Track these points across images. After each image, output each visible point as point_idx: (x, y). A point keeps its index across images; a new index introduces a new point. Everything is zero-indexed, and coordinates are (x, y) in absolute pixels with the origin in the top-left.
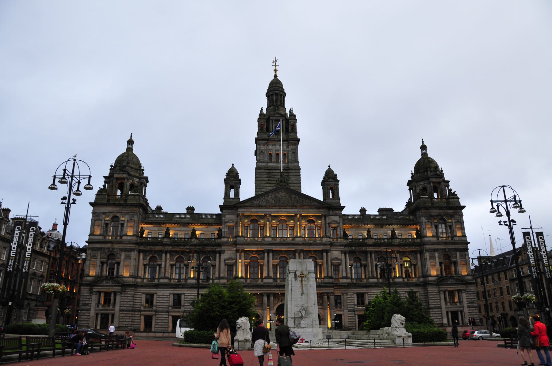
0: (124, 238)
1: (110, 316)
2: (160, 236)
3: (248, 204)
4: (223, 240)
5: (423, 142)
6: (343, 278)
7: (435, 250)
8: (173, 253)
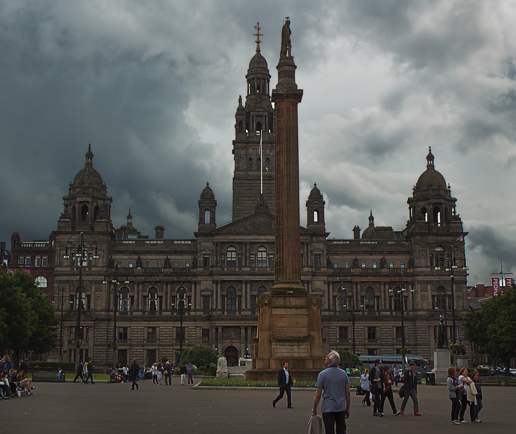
0: (93, 269)
1: (84, 351)
3: (225, 231)
5: (430, 150)
7: (429, 282)
8: (146, 284)
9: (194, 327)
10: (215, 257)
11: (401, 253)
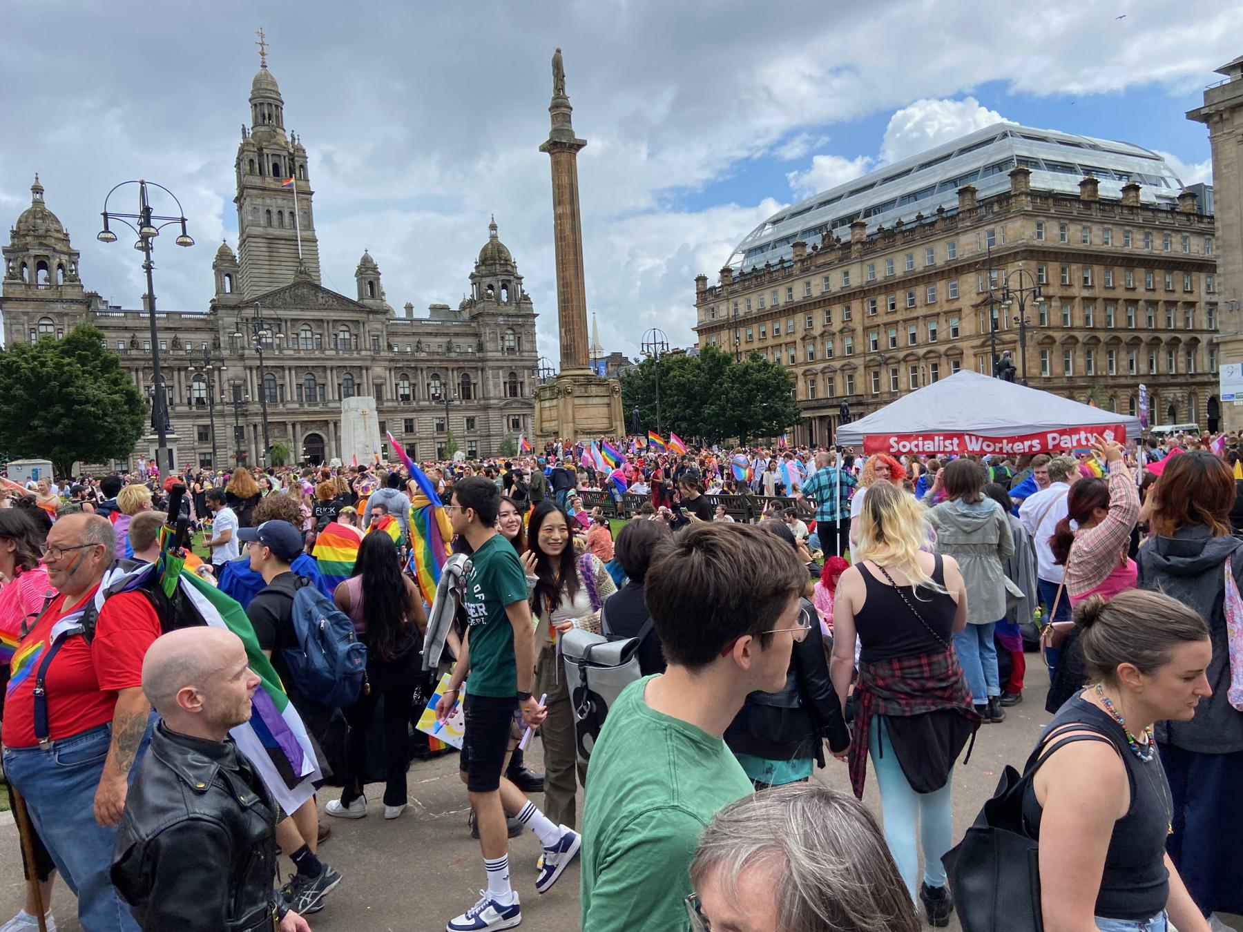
2: (121, 347)
11: (467, 335)
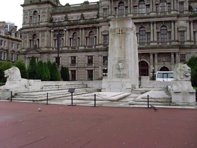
0: (41, 24)
4: (100, 19)
6: (188, 41)
9: (98, 56)
10: (110, 10)
